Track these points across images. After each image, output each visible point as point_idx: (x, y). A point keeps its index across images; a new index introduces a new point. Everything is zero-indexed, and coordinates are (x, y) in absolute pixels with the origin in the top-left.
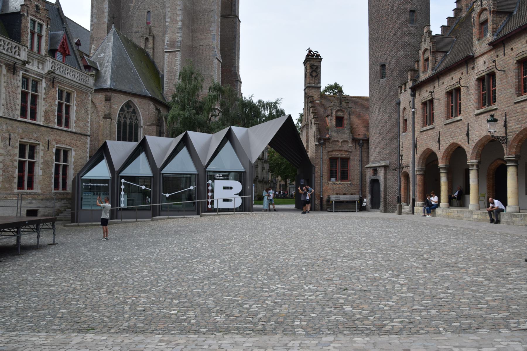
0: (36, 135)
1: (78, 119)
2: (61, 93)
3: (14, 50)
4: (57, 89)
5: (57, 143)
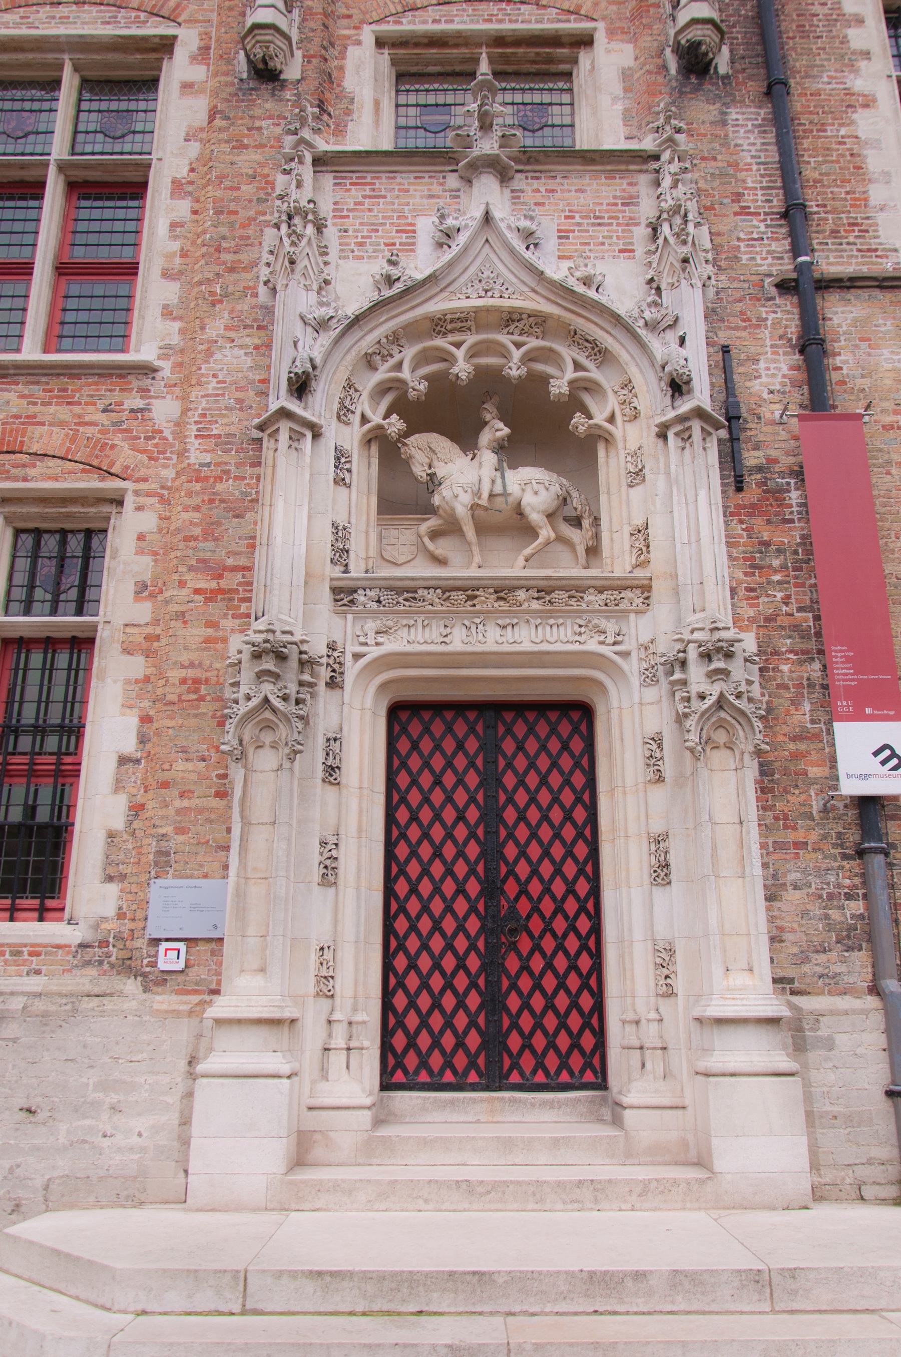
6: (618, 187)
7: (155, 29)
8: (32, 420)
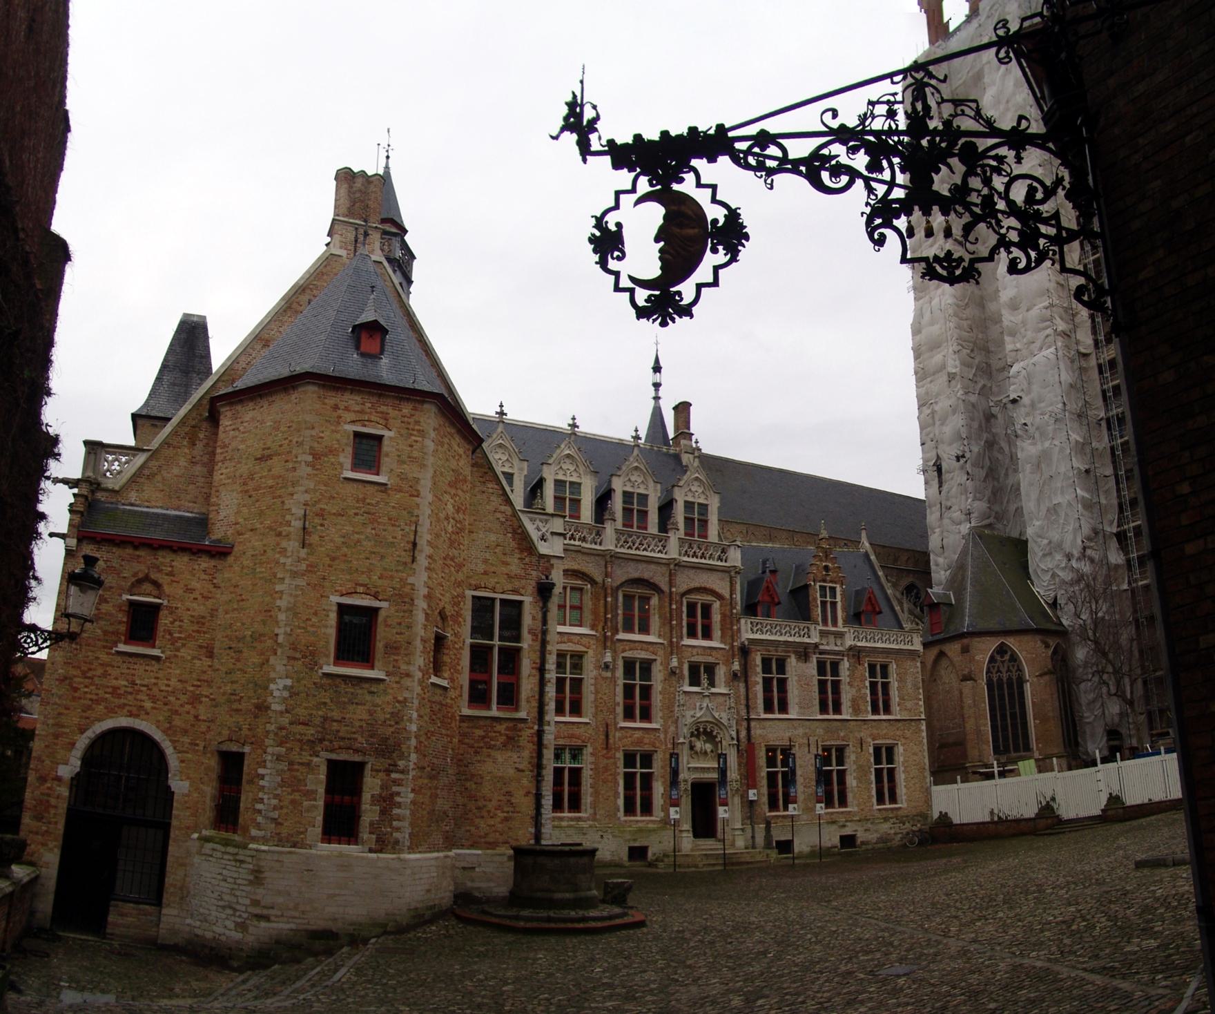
0: (842, 734)
1: (902, 698)
2: (872, 668)
3: (802, 633)
4: (866, 665)
5: (873, 740)
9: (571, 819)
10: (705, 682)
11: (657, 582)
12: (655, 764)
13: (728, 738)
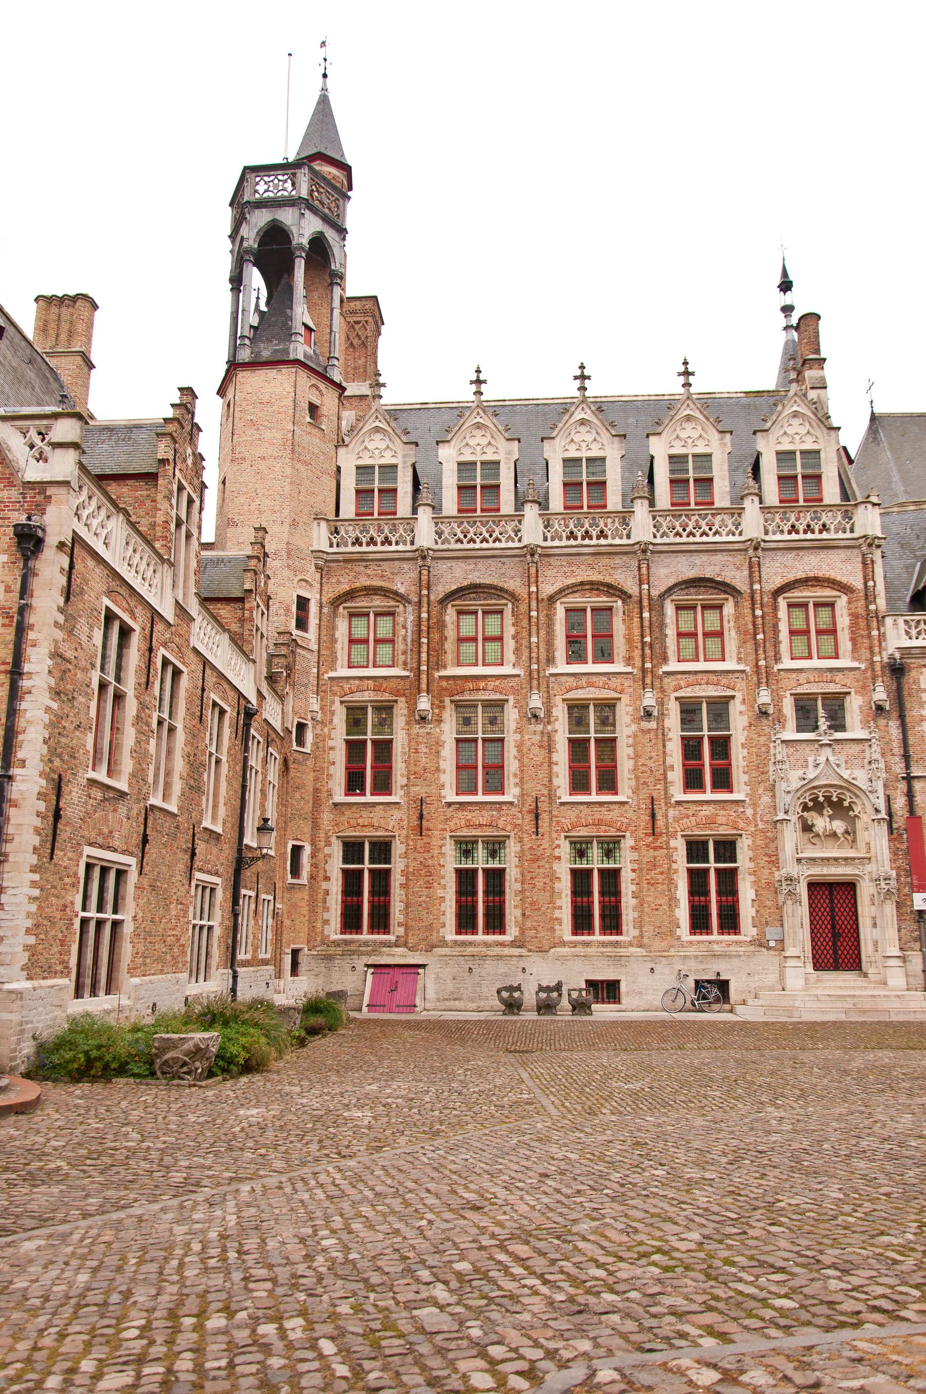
6: (860, 747)
7: (729, 693)
8: (717, 815)
9: (604, 944)
10: (823, 724)
11: (728, 580)
12: (739, 857)
13: (870, 810)
